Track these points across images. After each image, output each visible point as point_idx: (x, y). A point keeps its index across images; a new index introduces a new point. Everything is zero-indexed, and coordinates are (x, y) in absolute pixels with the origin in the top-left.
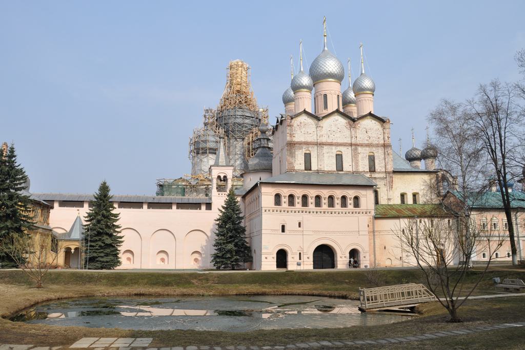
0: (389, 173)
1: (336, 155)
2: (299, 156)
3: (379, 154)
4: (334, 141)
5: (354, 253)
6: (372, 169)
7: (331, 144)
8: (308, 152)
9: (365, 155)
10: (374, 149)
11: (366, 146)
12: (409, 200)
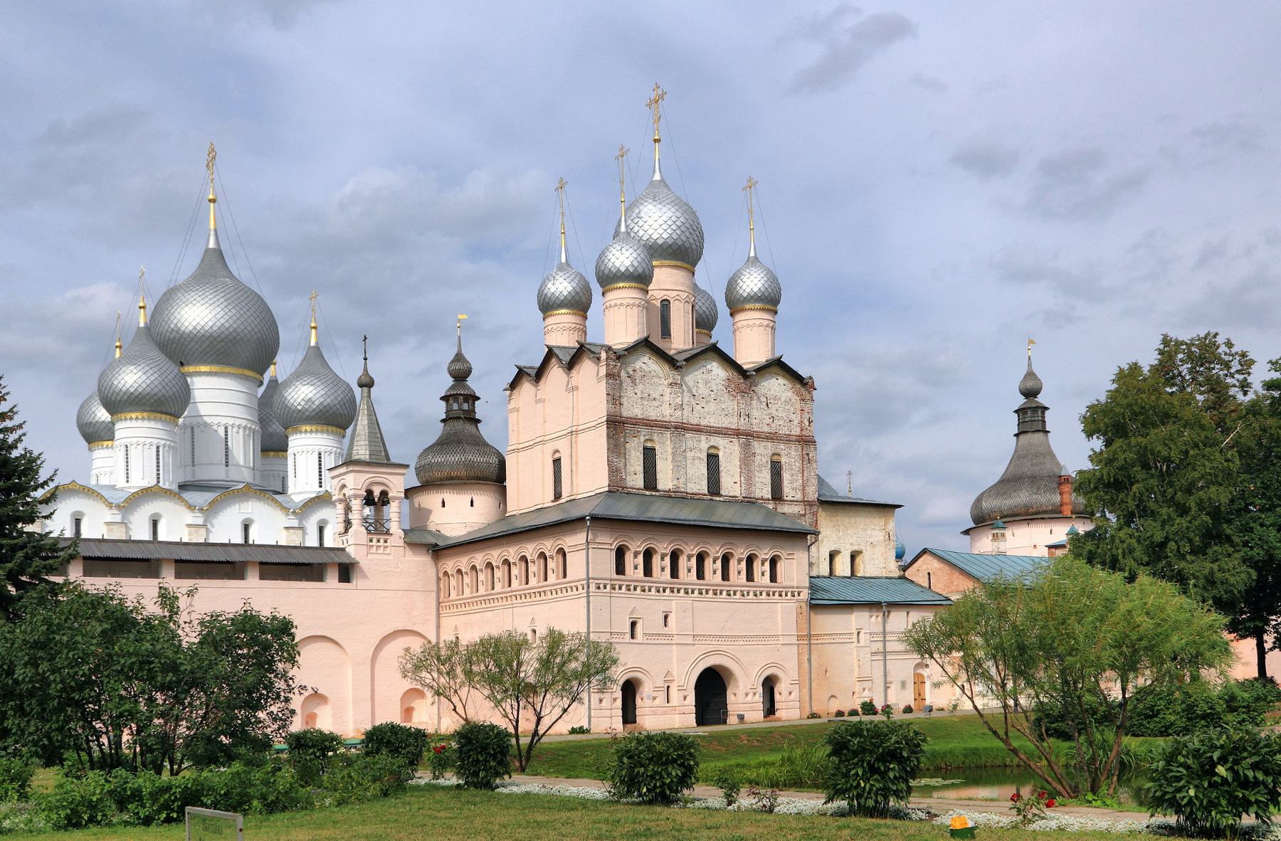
0: (810, 504)
1: (708, 455)
2: (633, 453)
3: (790, 458)
4: (704, 422)
6: (777, 495)
7: (698, 429)
8: (649, 445)
9: (764, 460)
10: (782, 446)
11: (767, 438)
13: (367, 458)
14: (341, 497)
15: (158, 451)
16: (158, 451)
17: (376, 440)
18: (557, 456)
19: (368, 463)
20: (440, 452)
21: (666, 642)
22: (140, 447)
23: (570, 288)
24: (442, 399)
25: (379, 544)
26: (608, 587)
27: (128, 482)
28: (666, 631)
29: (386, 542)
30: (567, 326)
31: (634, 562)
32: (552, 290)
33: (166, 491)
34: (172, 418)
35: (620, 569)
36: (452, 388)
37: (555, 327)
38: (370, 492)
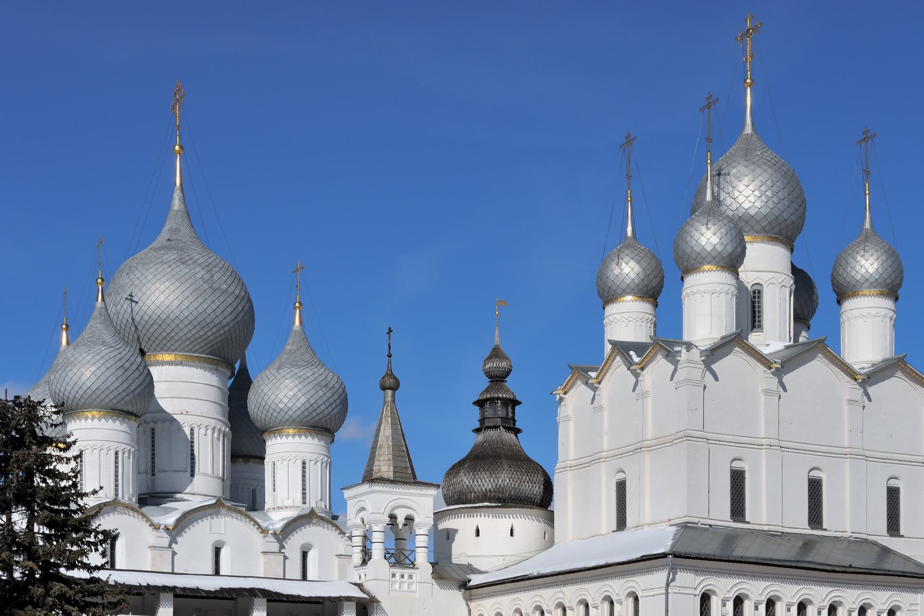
13: (390, 475)
14: (359, 522)
16: (117, 458)
17: (402, 453)
18: (621, 476)
22: (96, 452)
30: (635, 315)
34: (134, 418)
36: (487, 390)
37: (618, 317)
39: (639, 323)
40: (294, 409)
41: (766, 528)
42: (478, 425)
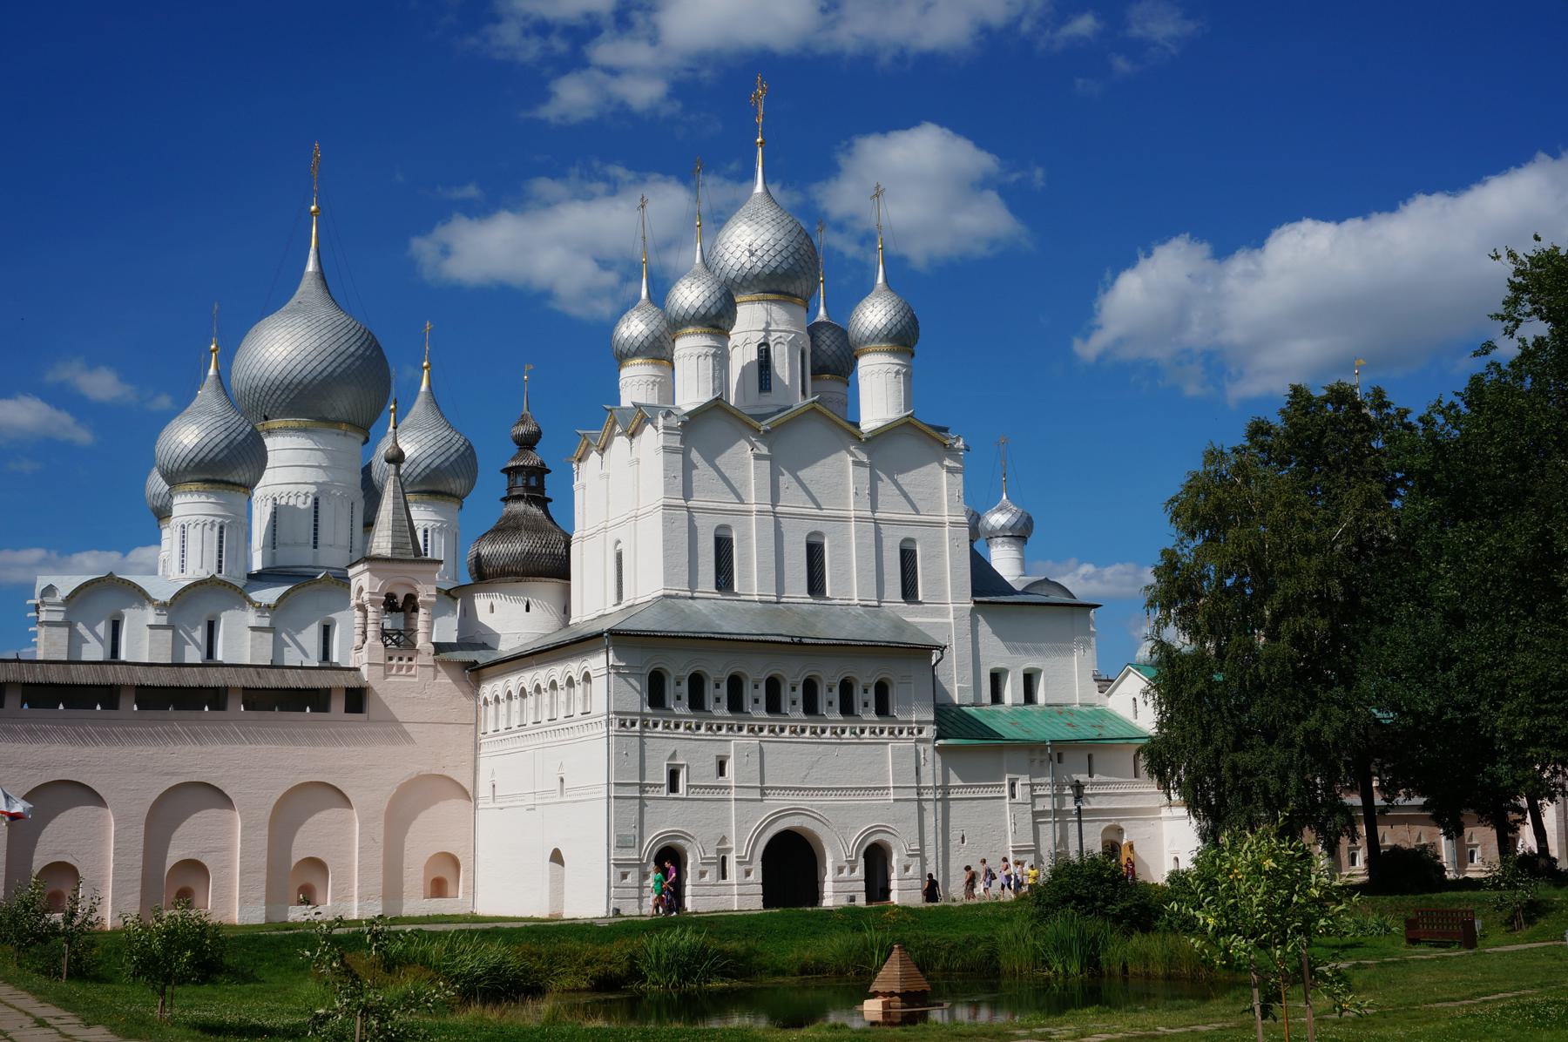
5: (876, 859)
12: (1012, 692)
15: (221, 532)
19: (387, 560)
20: (493, 541)
21: (720, 796)
22: (199, 527)
23: (646, 332)
24: (504, 471)
25: (400, 663)
26: (638, 724)
27: (183, 571)
28: (721, 781)
29: (410, 659)
31: (676, 691)
32: (626, 335)
33: (224, 583)
34: (242, 490)
35: (656, 697)
37: (629, 380)
38: (390, 597)
39: (650, 386)
40: (415, 474)
41: (756, 598)
42: (505, 494)
